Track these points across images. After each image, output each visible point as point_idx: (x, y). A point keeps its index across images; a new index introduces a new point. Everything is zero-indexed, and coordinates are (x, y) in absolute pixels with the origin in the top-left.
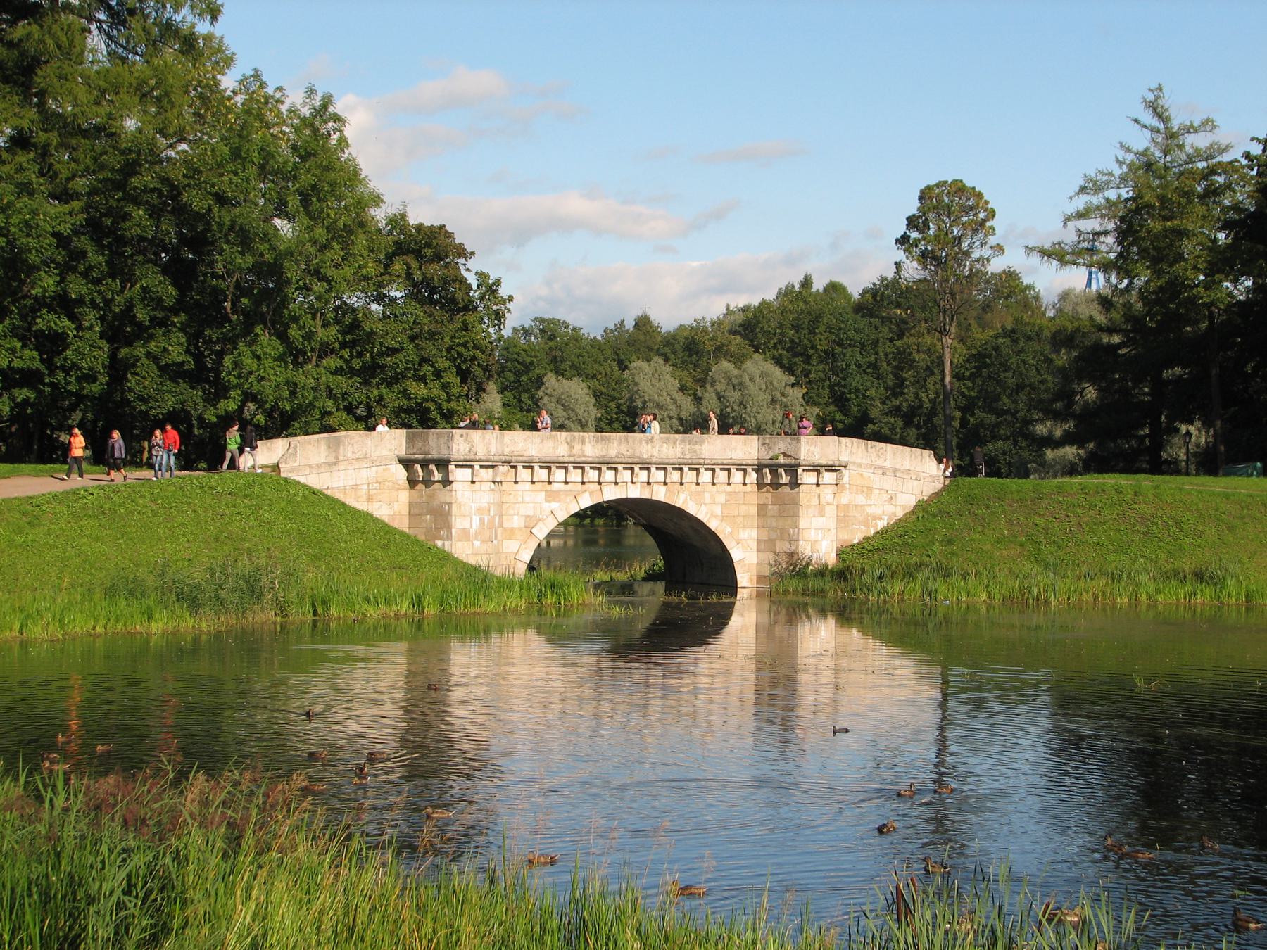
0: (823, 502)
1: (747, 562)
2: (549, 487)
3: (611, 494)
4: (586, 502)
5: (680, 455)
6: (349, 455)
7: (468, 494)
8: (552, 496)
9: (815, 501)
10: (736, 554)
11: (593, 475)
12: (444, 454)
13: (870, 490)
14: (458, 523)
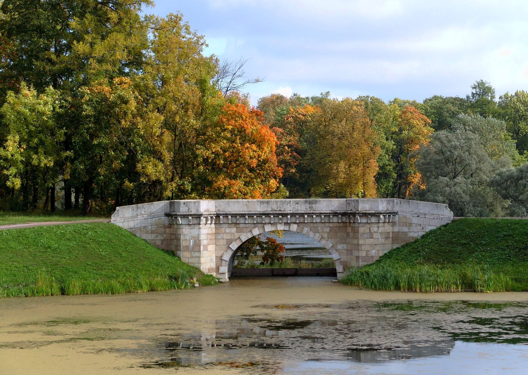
0: (372, 231)
1: (342, 260)
2: (238, 226)
5: (305, 210)
6: (143, 213)
7: (188, 230)
8: (240, 230)
9: (368, 231)
11: (259, 220)
13: (411, 224)
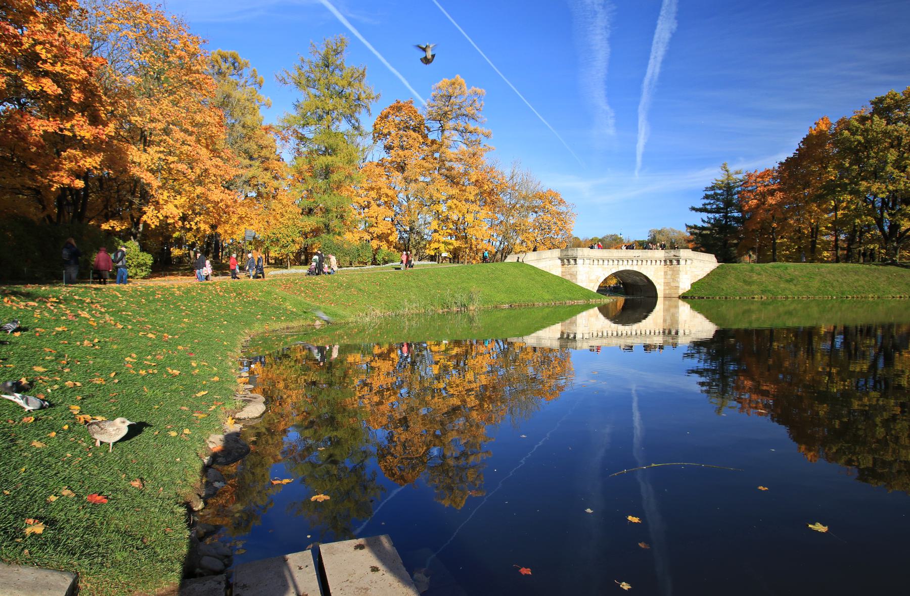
3: (621, 268)
4: (614, 271)
10: (658, 287)
12: (575, 255)
14: (579, 277)
